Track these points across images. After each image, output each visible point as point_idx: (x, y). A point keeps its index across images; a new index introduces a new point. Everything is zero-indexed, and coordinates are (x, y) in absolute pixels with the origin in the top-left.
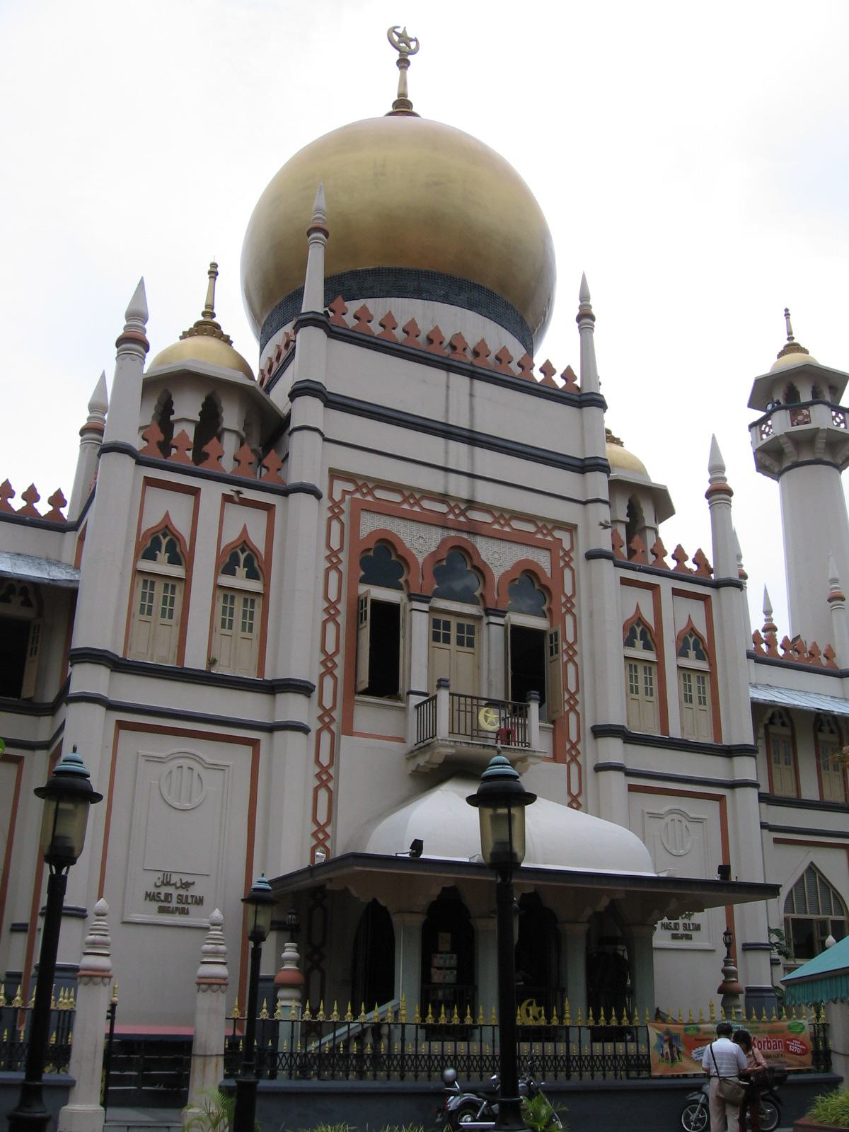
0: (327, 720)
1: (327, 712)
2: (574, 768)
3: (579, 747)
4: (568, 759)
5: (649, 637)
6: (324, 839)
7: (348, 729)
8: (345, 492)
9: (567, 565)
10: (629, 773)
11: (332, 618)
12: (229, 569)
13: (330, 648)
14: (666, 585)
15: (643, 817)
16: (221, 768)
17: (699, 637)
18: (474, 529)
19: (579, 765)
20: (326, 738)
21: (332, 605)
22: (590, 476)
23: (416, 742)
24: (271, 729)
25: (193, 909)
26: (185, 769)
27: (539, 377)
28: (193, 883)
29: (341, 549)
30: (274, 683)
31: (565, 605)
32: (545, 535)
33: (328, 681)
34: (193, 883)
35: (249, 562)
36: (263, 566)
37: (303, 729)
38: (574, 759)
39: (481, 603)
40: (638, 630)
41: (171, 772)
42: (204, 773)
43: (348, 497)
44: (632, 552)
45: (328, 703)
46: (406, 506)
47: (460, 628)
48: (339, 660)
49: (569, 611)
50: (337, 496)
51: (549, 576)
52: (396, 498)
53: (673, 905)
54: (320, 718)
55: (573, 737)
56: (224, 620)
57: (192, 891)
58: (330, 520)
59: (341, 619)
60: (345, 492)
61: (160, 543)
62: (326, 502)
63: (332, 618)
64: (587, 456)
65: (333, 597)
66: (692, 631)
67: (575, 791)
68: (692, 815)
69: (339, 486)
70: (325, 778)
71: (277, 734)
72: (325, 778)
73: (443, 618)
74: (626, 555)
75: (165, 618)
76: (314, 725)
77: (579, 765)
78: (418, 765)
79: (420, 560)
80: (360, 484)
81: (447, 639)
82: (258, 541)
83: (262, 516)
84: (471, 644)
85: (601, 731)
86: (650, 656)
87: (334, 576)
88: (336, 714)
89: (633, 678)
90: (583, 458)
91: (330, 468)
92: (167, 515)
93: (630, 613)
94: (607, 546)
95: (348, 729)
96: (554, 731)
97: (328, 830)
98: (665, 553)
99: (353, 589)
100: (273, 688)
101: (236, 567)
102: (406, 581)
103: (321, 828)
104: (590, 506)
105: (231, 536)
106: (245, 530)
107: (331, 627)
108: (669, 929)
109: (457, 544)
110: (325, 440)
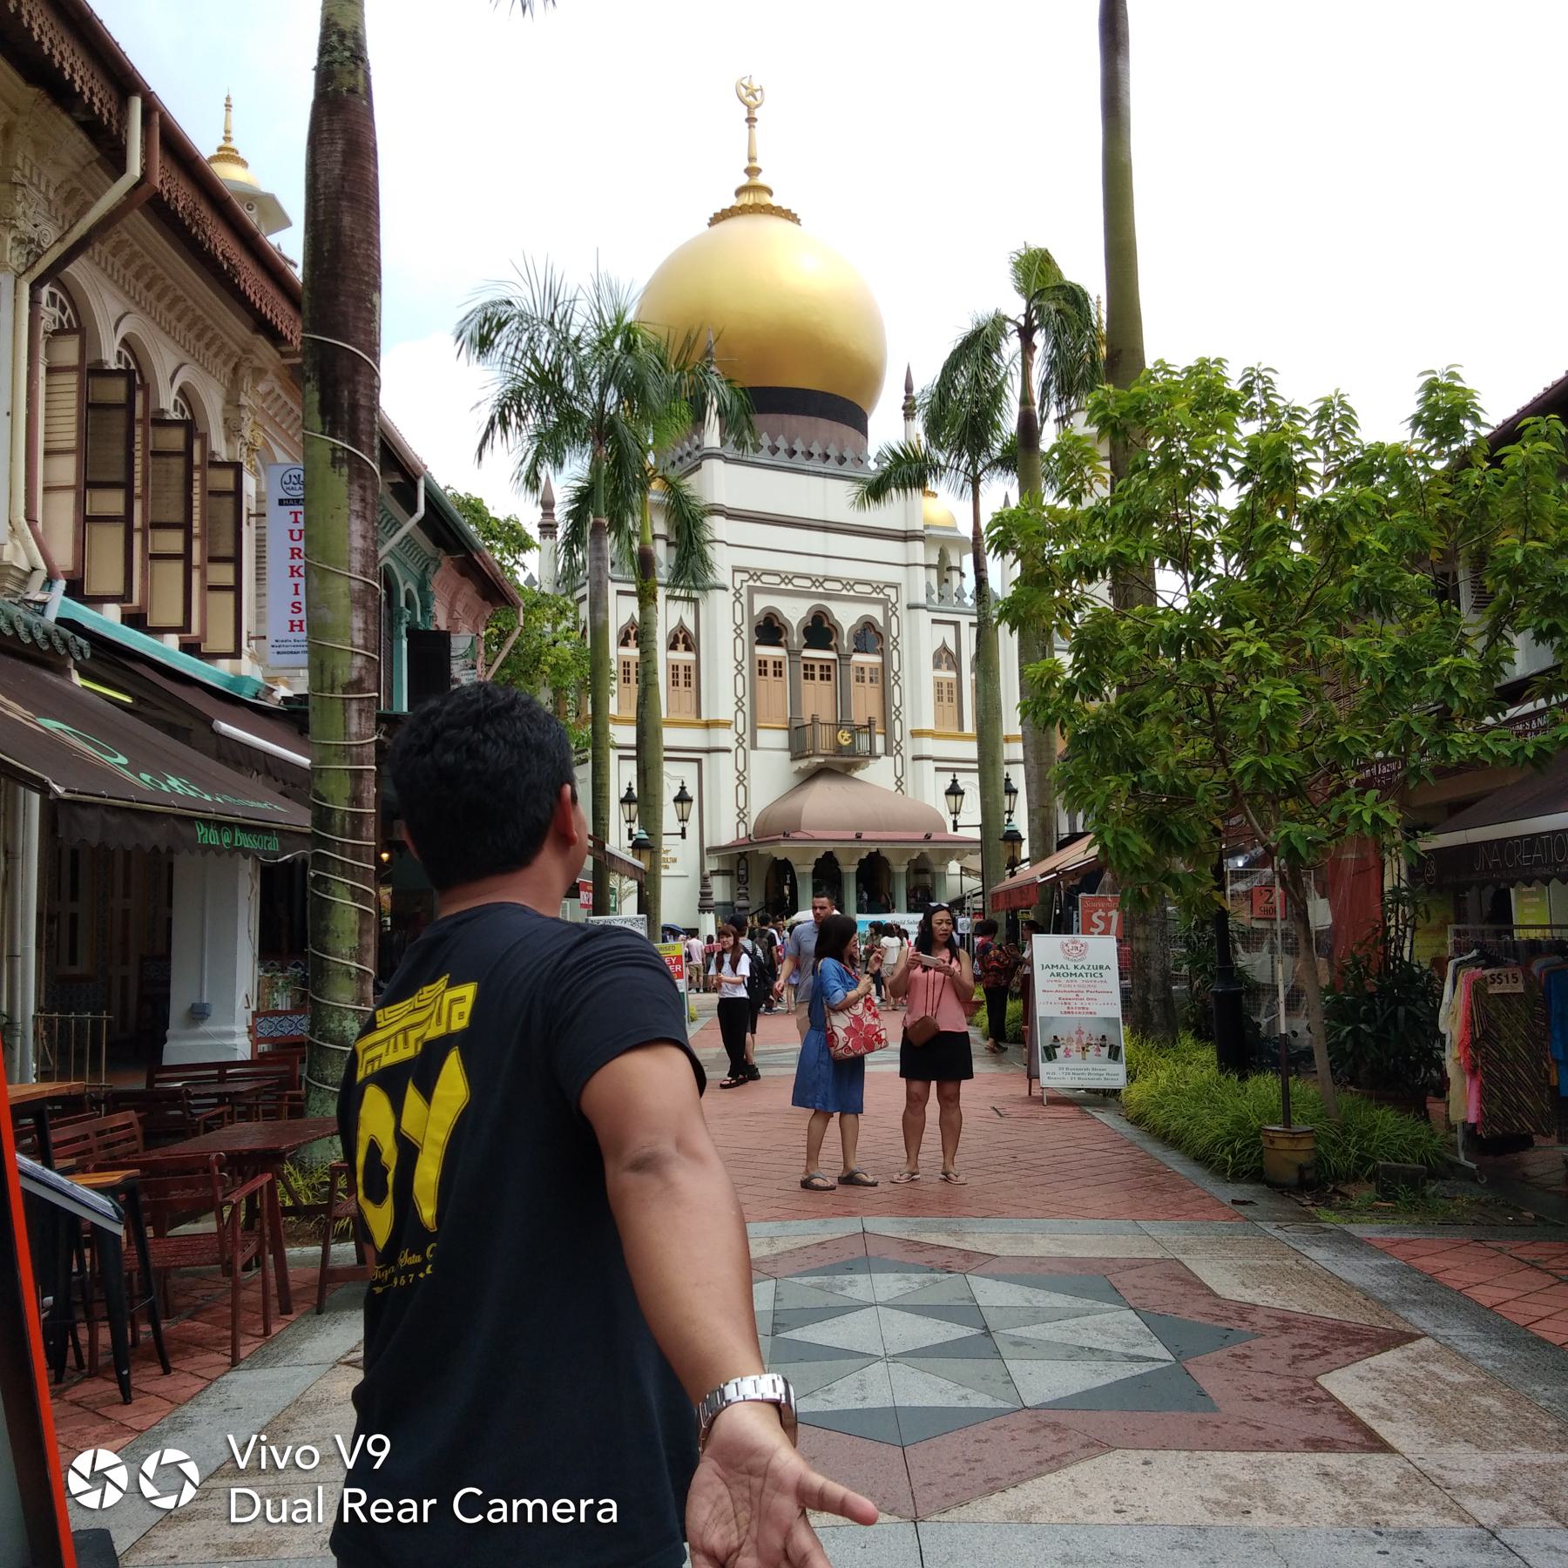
2: (898, 757)
10: (935, 760)
12: (673, 647)
18: (829, 596)
20: (740, 751)
21: (739, 663)
24: (708, 751)
33: (740, 714)
35: (685, 640)
37: (728, 751)
38: (898, 752)
44: (941, 597)
45: (740, 731)
47: (822, 667)
48: (746, 700)
49: (895, 648)
51: (882, 624)
52: (777, 580)
53: (958, 853)
55: (898, 738)
59: (746, 672)
67: (899, 775)
69: (740, 576)
70: (742, 778)
71: (713, 755)
72: (742, 778)
73: (809, 663)
76: (733, 746)
81: (813, 677)
82: (690, 626)
84: (829, 678)
85: (916, 734)
86: (953, 674)
87: (739, 641)
89: (940, 692)
93: (938, 645)
94: (922, 600)
95: (754, 746)
100: (708, 725)
103: (741, 811)
105: (673, 624)
106: (681, 619)
107: (739, 677)
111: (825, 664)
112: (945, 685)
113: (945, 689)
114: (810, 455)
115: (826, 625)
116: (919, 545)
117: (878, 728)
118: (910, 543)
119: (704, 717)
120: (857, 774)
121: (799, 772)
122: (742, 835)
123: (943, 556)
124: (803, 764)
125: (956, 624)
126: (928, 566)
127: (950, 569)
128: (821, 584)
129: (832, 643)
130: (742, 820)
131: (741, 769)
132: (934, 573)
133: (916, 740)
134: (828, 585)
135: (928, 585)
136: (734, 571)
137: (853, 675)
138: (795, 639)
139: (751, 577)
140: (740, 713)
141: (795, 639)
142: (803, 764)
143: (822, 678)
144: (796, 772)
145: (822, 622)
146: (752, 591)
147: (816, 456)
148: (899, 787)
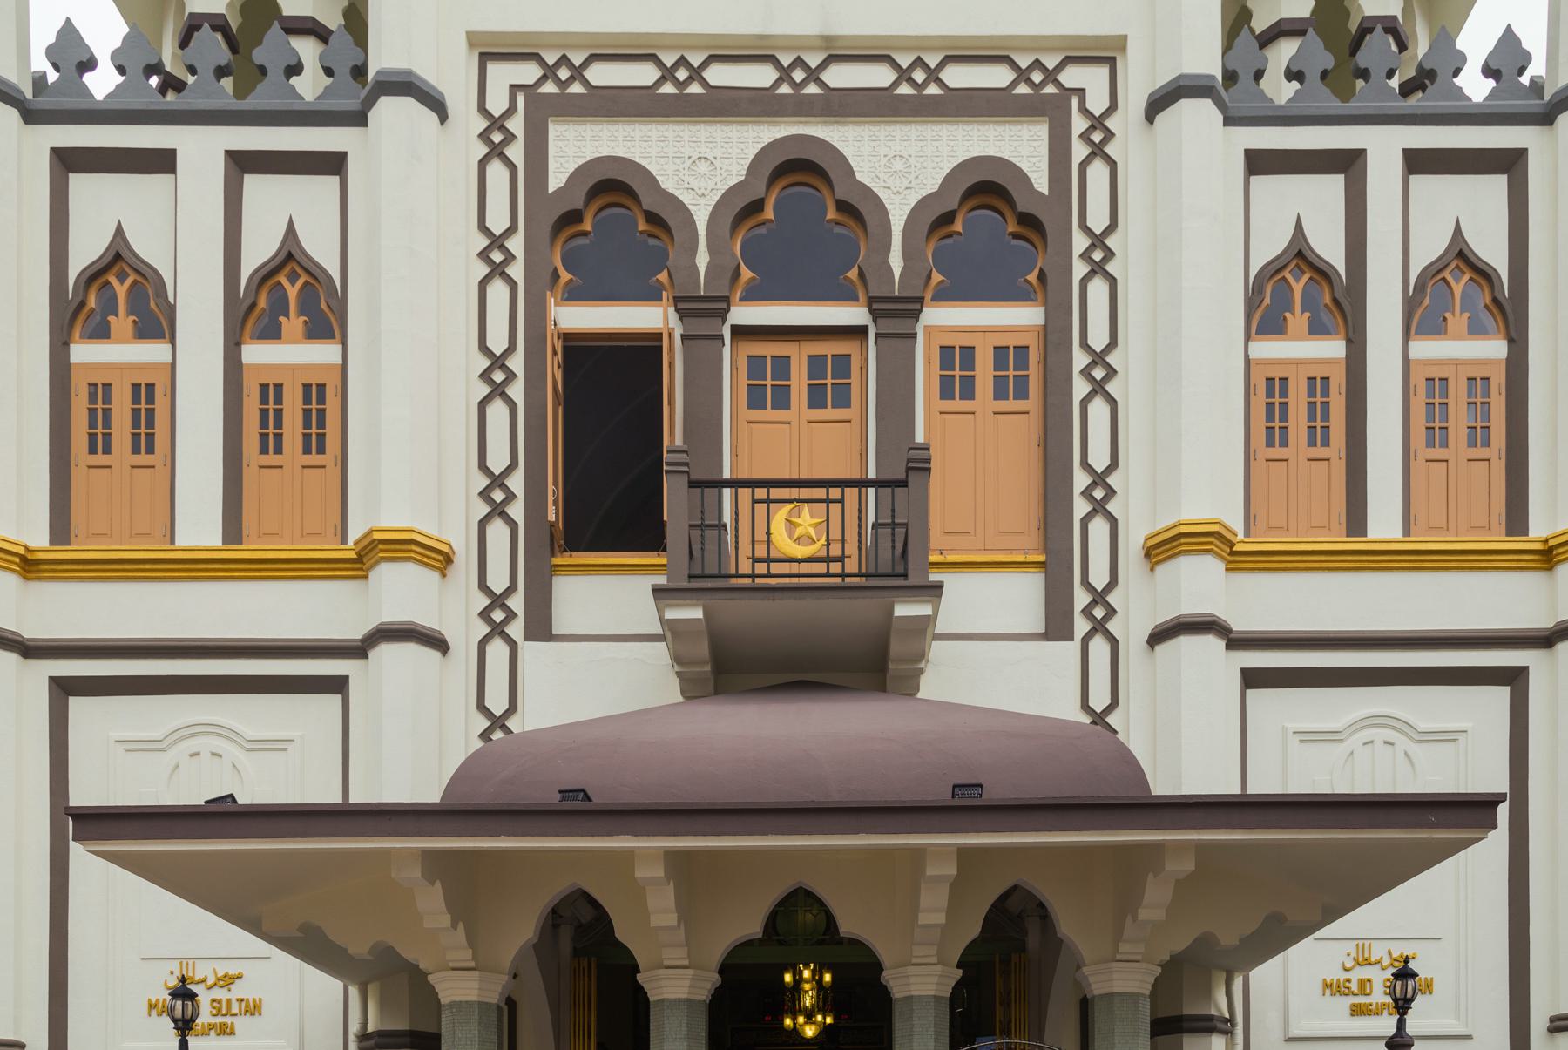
2: (1099, 646)
16: (278, 746)
20: (498, 652)
21: (498, 362)
25: (241, 1023)
26: (205, 755)
28: (239, 977)
34: (239, 977)
35: (308, 304)
38: (1099, 627)
41: (177, 766)
46: (668, 89)
47: (816, 363)
50: (497, 105)
56: (264, 437)
57: (238, 991)
61: (114, 297)
65: (498, 344)
68: (1423, 726)
69: (503, 76)
75: (139, 453)
79: (701, 217)
80: (551, 62)
82: (321, 248)
84: (843, 400)
86: (1333, 348)
91: (468, 34)
92: (119, 231)
96: (1046, 573)
101: (282, 319)
106: (291, 230)
108: (1347, 995)
113: (1298, 399)
136: (485, 58)
143: (816, 398)
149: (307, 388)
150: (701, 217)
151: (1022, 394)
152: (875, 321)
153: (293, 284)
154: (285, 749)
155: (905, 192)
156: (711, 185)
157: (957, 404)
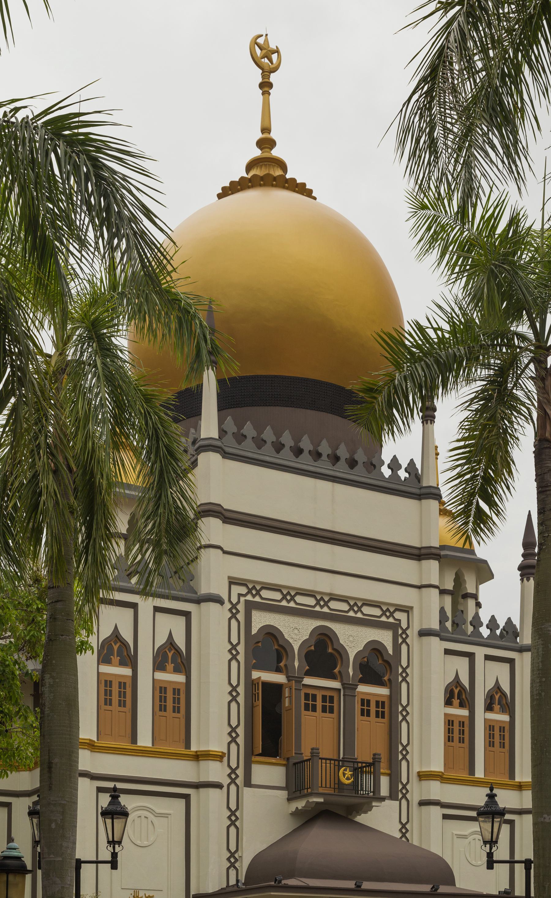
0: (233, 776)
1: (233, 771)
2: (404, 802)
3: (408, 787)
4: (400, 796)
5: (464, 697)
6: (235, 862)
7: (248, 783)
8: (240, 595)
9: (404, 641)
11: (234, 699)
13: (234, 723)
14: (480, 652)
15: (453, 838)
16: (165, 816)
17: (504, 694)
19: (408, 801)
21: (234, 689)
22: (425, 563)
23: (294, 791)
24: (197, 786)
26: (143, 817)
27: (386, 472)
29: (238, 643)
30: (198, 753)
31: (401, 674)
32: (388, 617)
33: (233, 746)
36: (185, 662)
37: (219, 786)
38: (404, 796)
39: (339, 678)
40: (456, 691)
42: (155, 820)
43: (242, 599)
45: (234, 765)
47: (324, 698)
48: (241, 731)
49: (404, 679)
50: (234, 600)
51: (391, 652)
52: (278, 596)
54: (229, 775)
55: (404, 780)
58: (230, 619)
59: (241, 699)
60: (240, 595)
62: (228, 606)
63: (234, 699)
64: (423, 546)
65: (234, 682)
66: (497, 687)
67: (404, 820)
69: (237, 590)
73: (311, 692)
74: (450, 629)
76: (225, 781)
77: (408, 801)
78: (297, 808)
79: (296, 648)
81: (314, 709)
82: (181, 643)
83: (182, 620)
86: (465, 712)
87: (234, 664)
88: (238, 772)
90: (418, 545)
91: (228, 577)
94: (435, 626)
95: (248, 783)
97: (236, 855)
98: (481, 624)
99: (248, 675)
100: (198, 757)
102: (286, 665)
103: (232, 855)
104: (424, 590)
106: (170, 634)
107: (234, 705)
109: (322, 632)
110: (225, 552)
111: (328, 693)
112: (456, 724)
113: (456, 728)
114: (317, 455)
115: (330, 650)
116: (434, 565)
117: (383, 768)
118: (424, 562)
119: (194, 748)
120: (361, 819)
121: (296, 814)
122: (232, 882)
123: (459, 581)
124: (300, 804)
125: (471, 656)
126: (443, 592)
127: (466, 596)
128: (326, 604)
129: (336, 671)
130: (233, 865)
131: (233, 807)
132: (448, 599)
133: (424, 783)
134: (334, 605)
135: (442, 611)
137: (358, 707)
138: (296, 664)
139: (249, 592)
140: (233, 745)
141: (296, 664)
142: (300, 804)
143: (324, 710)
144: (293, 814)
145: (326, 647)
146: (250, 606)
147: (324, 457)
148: (404, 835)
149: (174, 689)
150: (296, 648)
151: (383, 717)
152: (344, 688)
153: (170, 652)
154: (167, 817)
155: (353, 648)
156: (298, 637)
157: (365, 718)
